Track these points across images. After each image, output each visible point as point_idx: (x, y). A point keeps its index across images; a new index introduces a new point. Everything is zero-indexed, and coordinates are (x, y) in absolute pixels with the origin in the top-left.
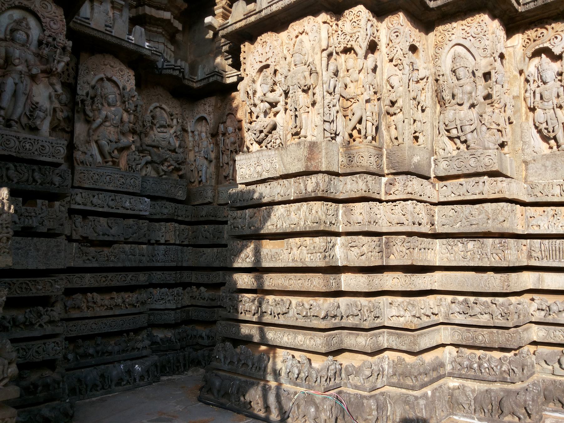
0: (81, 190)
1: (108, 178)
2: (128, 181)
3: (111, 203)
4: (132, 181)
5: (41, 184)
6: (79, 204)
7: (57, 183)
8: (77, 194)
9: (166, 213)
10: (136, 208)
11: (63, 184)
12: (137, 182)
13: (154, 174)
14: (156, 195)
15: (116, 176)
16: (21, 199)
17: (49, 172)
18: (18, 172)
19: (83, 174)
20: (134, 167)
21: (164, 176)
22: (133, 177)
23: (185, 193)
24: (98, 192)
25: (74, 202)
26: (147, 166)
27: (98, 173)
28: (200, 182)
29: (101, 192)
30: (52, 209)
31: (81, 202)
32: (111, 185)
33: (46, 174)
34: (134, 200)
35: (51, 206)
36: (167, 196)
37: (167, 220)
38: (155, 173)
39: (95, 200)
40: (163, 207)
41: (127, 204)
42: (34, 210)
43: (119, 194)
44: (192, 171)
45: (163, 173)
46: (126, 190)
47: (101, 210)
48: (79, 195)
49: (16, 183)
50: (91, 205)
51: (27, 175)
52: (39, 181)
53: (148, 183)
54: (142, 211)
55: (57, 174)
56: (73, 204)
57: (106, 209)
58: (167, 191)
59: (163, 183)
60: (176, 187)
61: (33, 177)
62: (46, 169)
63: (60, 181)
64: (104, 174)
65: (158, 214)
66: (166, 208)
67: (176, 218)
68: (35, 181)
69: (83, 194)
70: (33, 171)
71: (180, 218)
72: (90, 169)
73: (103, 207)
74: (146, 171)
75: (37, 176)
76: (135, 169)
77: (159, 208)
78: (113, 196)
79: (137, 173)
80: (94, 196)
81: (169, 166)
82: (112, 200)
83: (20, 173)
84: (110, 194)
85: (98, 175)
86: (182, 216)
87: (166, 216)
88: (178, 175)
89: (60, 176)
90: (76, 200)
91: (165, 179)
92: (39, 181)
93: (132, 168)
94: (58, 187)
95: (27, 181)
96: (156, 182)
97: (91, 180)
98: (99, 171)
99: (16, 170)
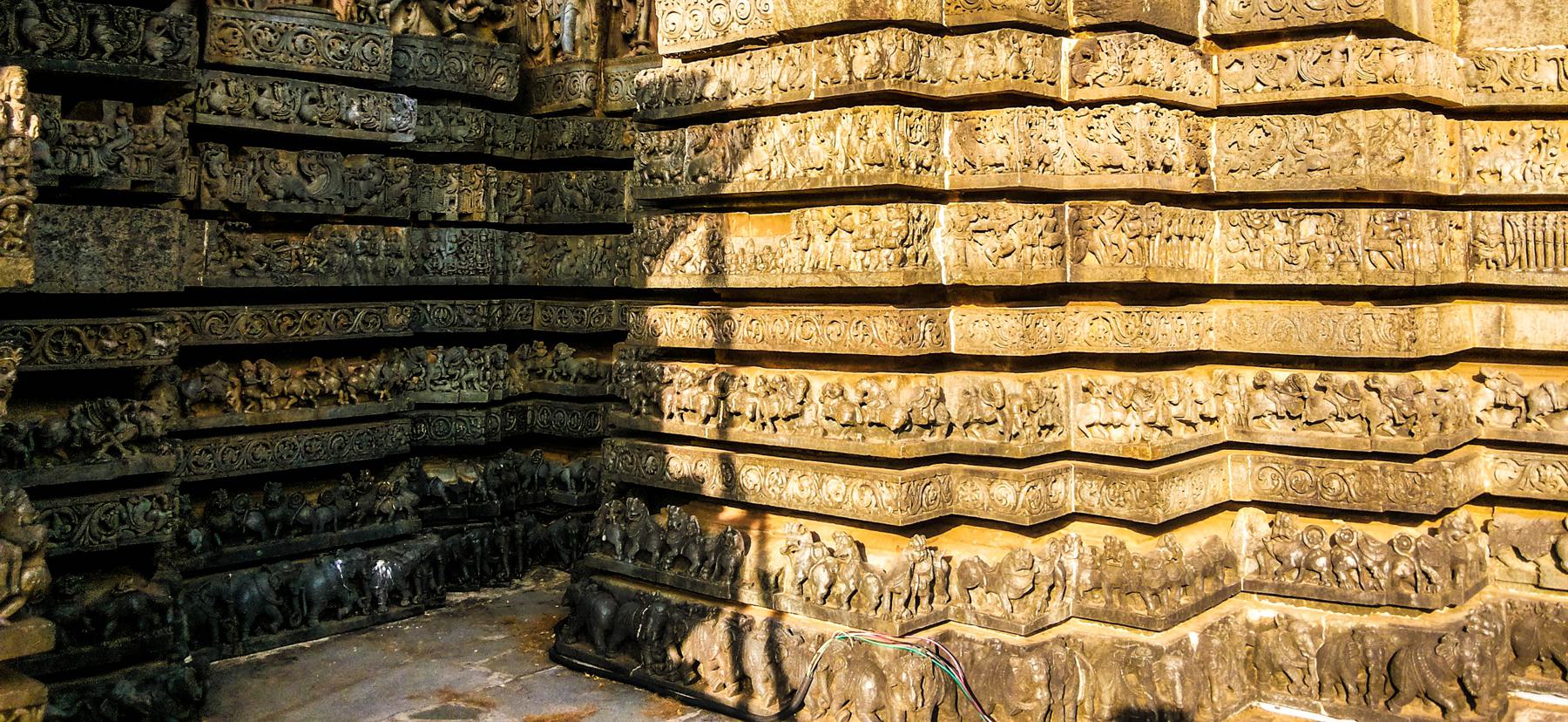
0: (224, 75)
1: (300, 40)
2: (356, 49)
3: (308, 110)
4: (367, 48)
5: (114, 57)
6: (219, 113)
7: (159, 55)
8: (214, 86)
9: (460, 139)
10: (378, 123)
11: (175, 58)
12: (381, 52)
13: (426, 29)
14: (433, 85)
15: (322, 34)
16: (57, 99)
17: (137, 25)
18: (50, 22)
19: (230, 30)
20: (371, 8)
21: (456, 36)
22: (368, 37)
23: (515, 82)
24: (272, 79)
25: (206, 107)
26: (410, 7)
27: (272, 25)
28: (556, 51)
29: (279, 79)
30: (146, 127)
31: (224, 108)
32: (308, 60)
33: (126, 27)
34: (371, 100)
35: (142, 118)
36: (463, 89)
37: (464, 158)
38: (432, 26)
39: (264, 102)
40: (454, 122)
41: (354, 113)
42: (96, 129)
43: (331, 86)
44: (534, 20)
45: (451, 27)
46: (350, 73)
47: (280, 128)
48: (220, 88)
49: (46, 54)
50: (253, 115)
51: (74, 31)
52: (109, 48)
53: (412, 55)
54: (394, 131)
55: (159, 29)
56: (202, 112)
57: (295, 127)
58: (465, 76)
59: (454, 54)
60: (488, 66)
61: (92, 37)
62: (127, 15)
63: (167, 47)
64: (290, 28)
65: (441, 140)
66: (461, 122)
67: (488, 150)
68: (96, 47)
69: (232, 85)
70: (93, 20)
71: (499, 153)
72: (251, 15)
73: (286, 121)
74: (406, 21)
75: (103, 33)
76: (374, 15)
77: (441, 124)
78: (315, 89)
79: (380, 27)
80: (261, 91)
81: (469, 7)
82: (312, 101)
83: (56, 27)
84: (304, 83)
85: (272, 31)
86: (506, 145)
87: (461, 145)
88: (496, 33)
89: (168, 35)
90: (212, 100)
91: (457, 42)
92: (109, 48)
93: (367, 12)
94: (162, 65)
95: (75, 48)
96: (433, 52)
97: (253, 46)
98: (275, 19)
99: (45, 18)
